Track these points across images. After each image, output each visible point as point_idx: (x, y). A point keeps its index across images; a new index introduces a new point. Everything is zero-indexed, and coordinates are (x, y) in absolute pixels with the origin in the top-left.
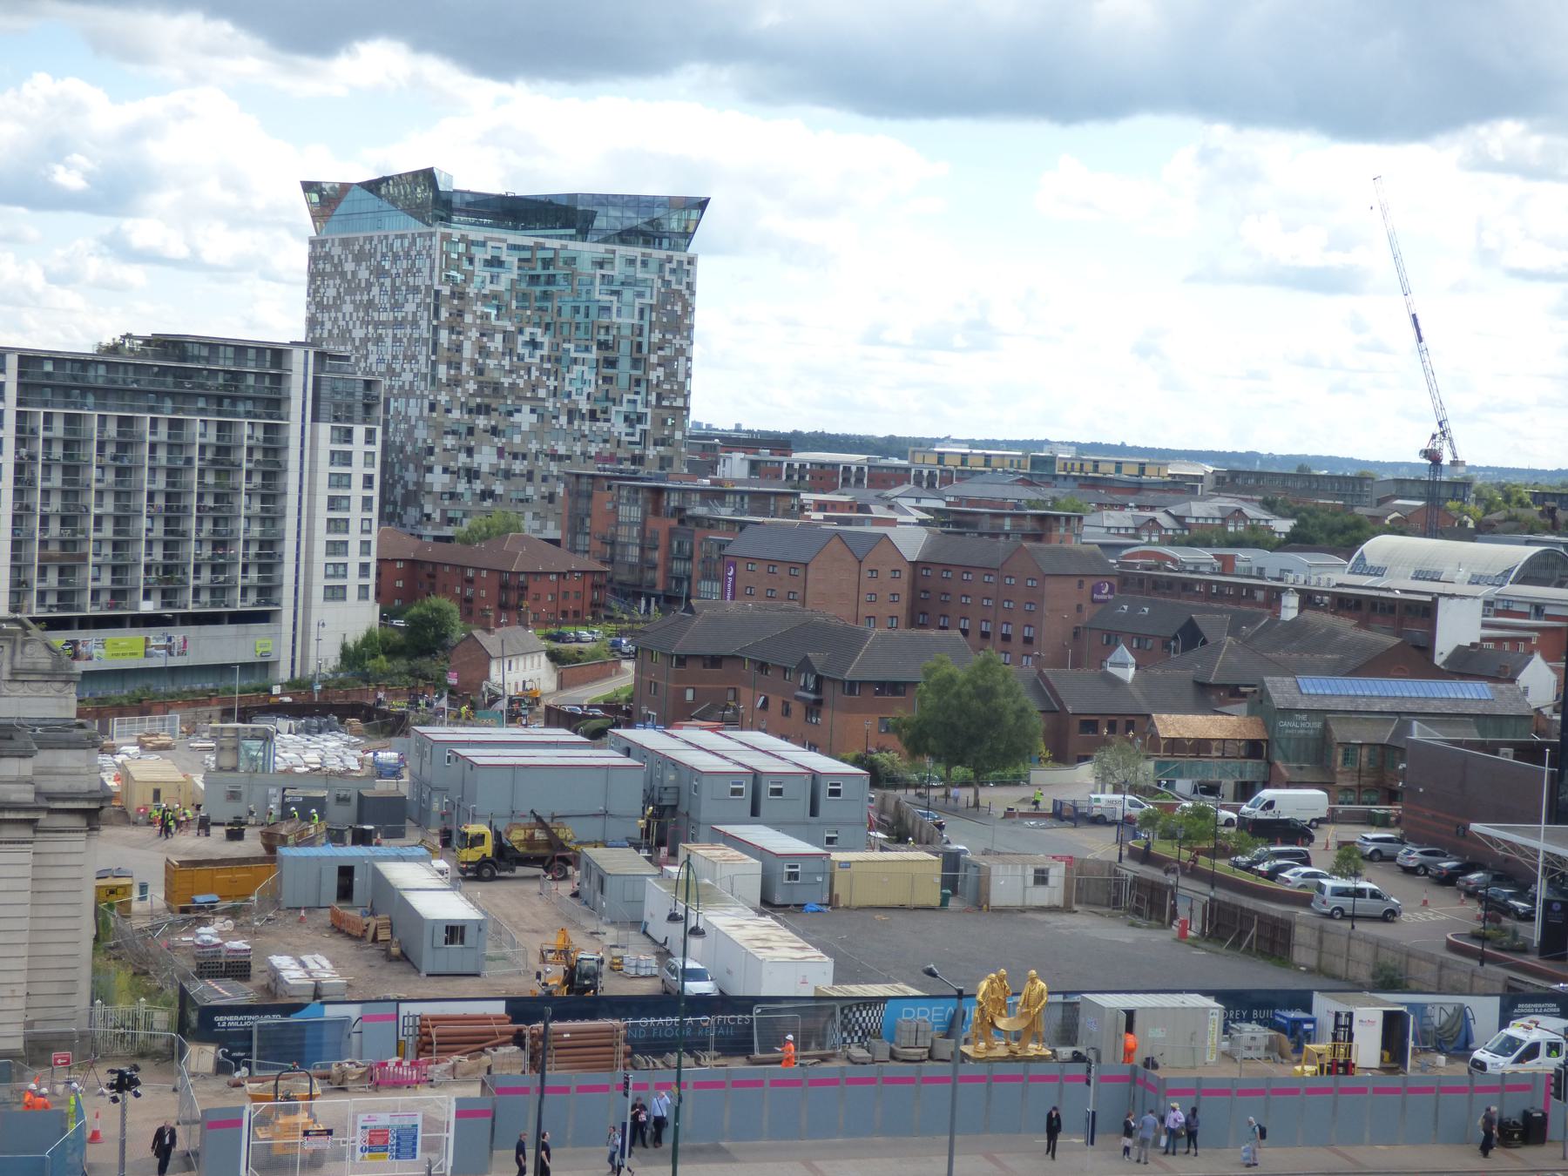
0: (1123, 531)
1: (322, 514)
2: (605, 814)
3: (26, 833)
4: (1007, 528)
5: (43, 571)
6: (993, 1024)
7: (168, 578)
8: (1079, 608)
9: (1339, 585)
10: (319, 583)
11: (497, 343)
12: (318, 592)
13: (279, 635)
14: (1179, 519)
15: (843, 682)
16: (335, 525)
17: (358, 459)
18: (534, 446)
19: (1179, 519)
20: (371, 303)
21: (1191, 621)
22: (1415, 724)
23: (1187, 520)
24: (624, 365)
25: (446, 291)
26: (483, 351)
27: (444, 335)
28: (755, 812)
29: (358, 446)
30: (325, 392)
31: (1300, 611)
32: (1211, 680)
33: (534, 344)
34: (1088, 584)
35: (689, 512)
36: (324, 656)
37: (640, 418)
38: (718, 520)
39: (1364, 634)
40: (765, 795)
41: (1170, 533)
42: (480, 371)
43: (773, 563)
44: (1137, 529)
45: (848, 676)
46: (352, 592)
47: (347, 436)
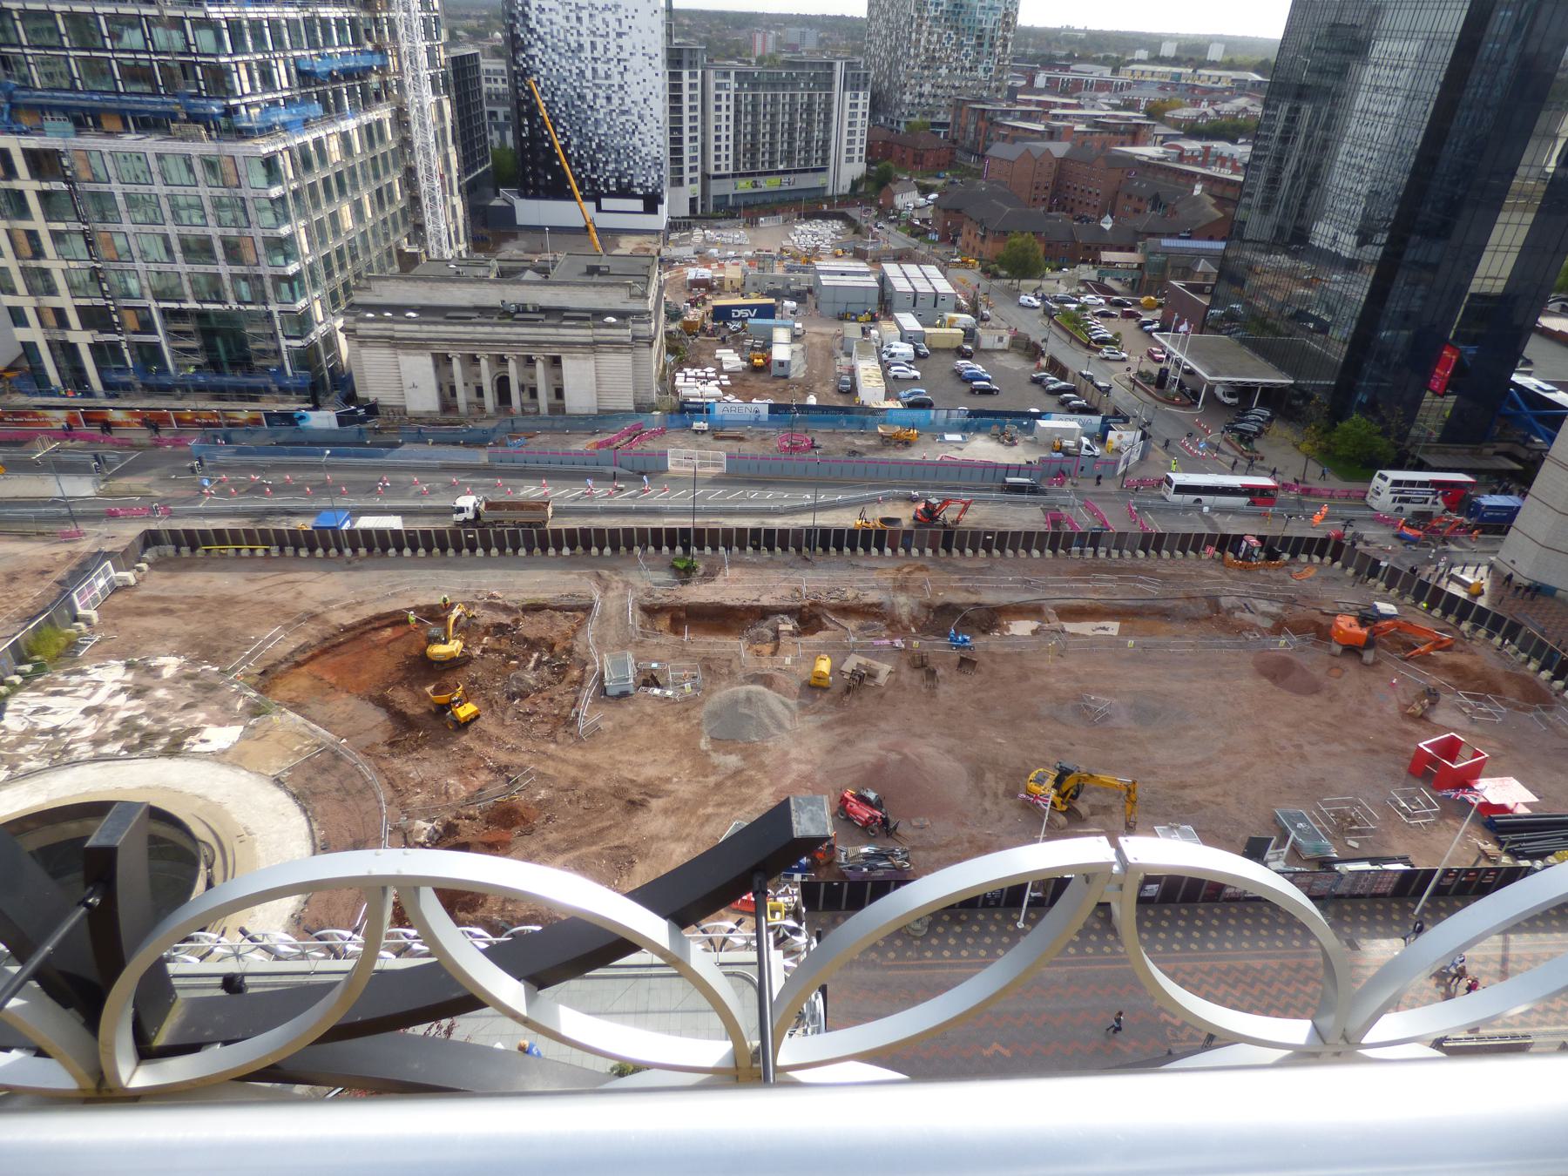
1: (846, 128)
5: (744, 155)
7: (789, 156)
10: (844, 155)
11: (935, 38)
13: (827, 177)
16: (851, 133)
17: (860, 105)
18: (946, 83)
20: (888, 21)
24: (986, 45)
25: (916, 15)
26: (929, 42)
27: (914, 35)
29: (860, 101)
30: (849, 78)
33: (950, 38)
34: (1126, 171)
36: (844, 186)
37: (990, 69)
40: (918, 300)
42: (927, 50)
43: (1003, 160)
46: (856, 159)
47: (857, 96)
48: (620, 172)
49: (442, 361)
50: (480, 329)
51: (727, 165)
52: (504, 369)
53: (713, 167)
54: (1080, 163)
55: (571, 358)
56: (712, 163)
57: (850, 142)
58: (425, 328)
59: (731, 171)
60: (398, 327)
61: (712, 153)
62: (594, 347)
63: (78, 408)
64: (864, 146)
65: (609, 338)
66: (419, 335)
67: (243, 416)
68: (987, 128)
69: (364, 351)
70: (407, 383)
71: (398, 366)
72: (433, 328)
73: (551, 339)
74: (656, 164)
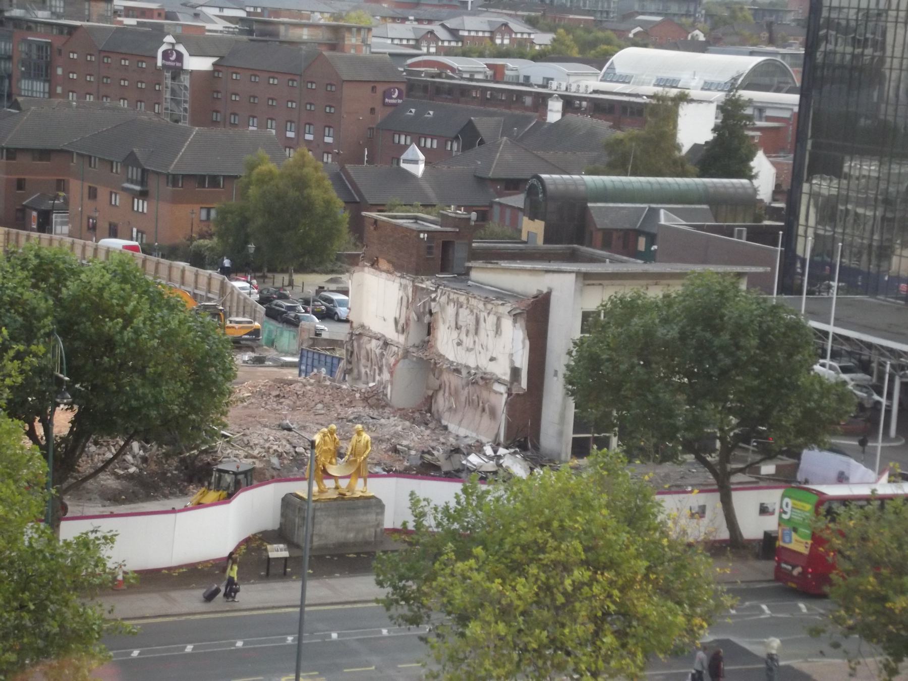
0: (405, 42)
4: (305, 37)
6: (324, 471)
8: (373, 110)
9: (595, 92)
14: (454, 32)
15: (168, 175)
19: (454, 32)
21: (470, 122)
22: (662, 212)
23: (461, 33)
31: (563, 115)
32: (490, 175)
34: (381, 88)
35: (7, 14)
38: (36, 23)
41: (446, 44)
44: (417, 40)
45: (171, 169)
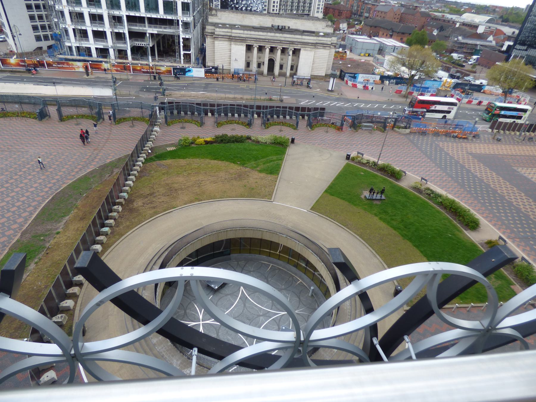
2: (374, 50)
3: (329, 48)
10: (316, 10)
12: (316, 12)
28: (394, 51)
39: (472, 31)
46: (320, 12)
48: (247, 5)
49: (249, 48)
50: (269, 34)
51: (276, 10)
52: (272, 55)
53: (272, 10)
54: (409, 15)
55: (305, 50)
56: (272, 8)
57: (319, 5)
58: (246, 32)
59: (278, 12)
60: (234, 31)
61: (272, 4)
62: (315, 45)
63: (88, 61)
64: (323, 7)
65: (322, 42)
66: (242, 36)
67: (163, 69)
68: (362, 5)
69: (216, 43)
70: (233, 58)
71: (230, 50)
72: (249, 32)
73: (299, 40)
74: (262, 2)
